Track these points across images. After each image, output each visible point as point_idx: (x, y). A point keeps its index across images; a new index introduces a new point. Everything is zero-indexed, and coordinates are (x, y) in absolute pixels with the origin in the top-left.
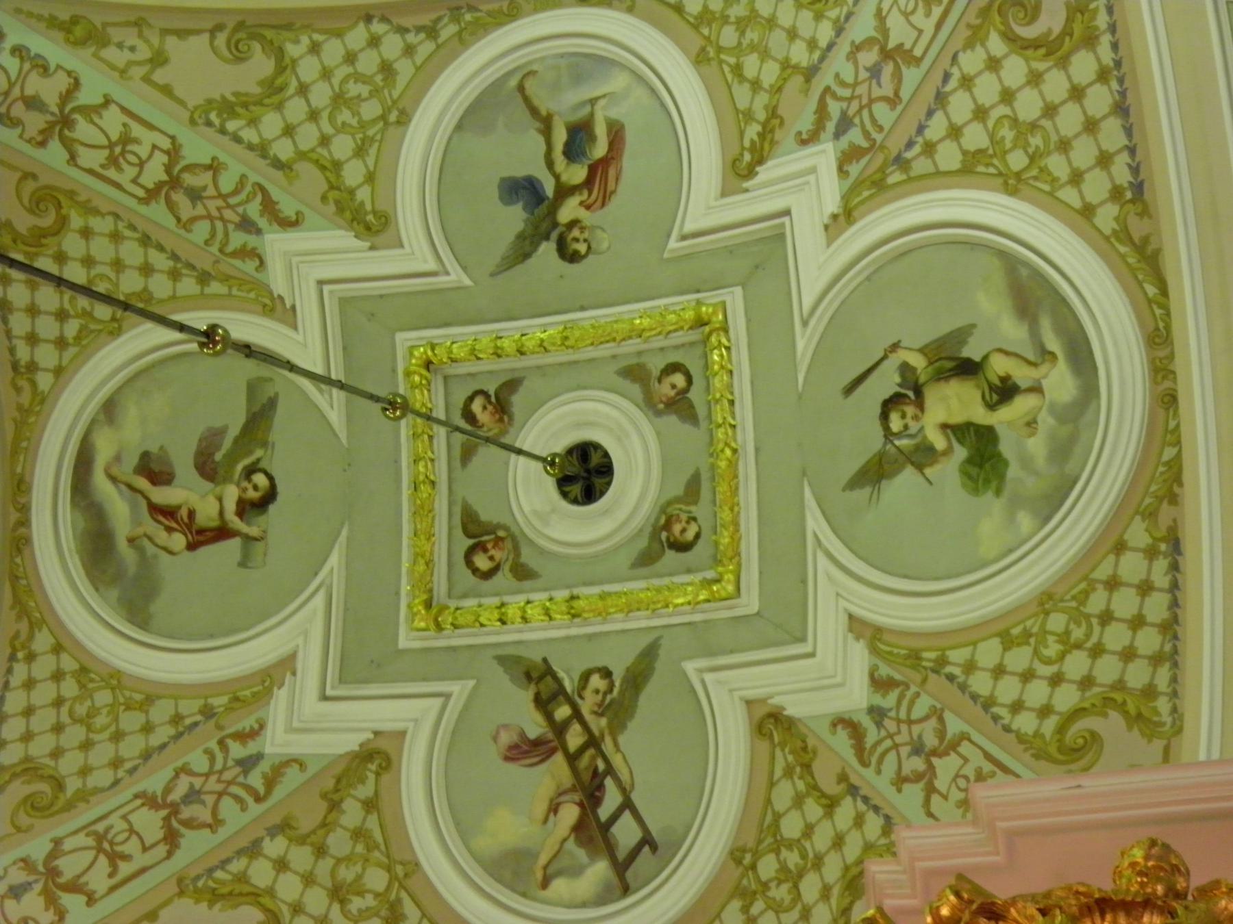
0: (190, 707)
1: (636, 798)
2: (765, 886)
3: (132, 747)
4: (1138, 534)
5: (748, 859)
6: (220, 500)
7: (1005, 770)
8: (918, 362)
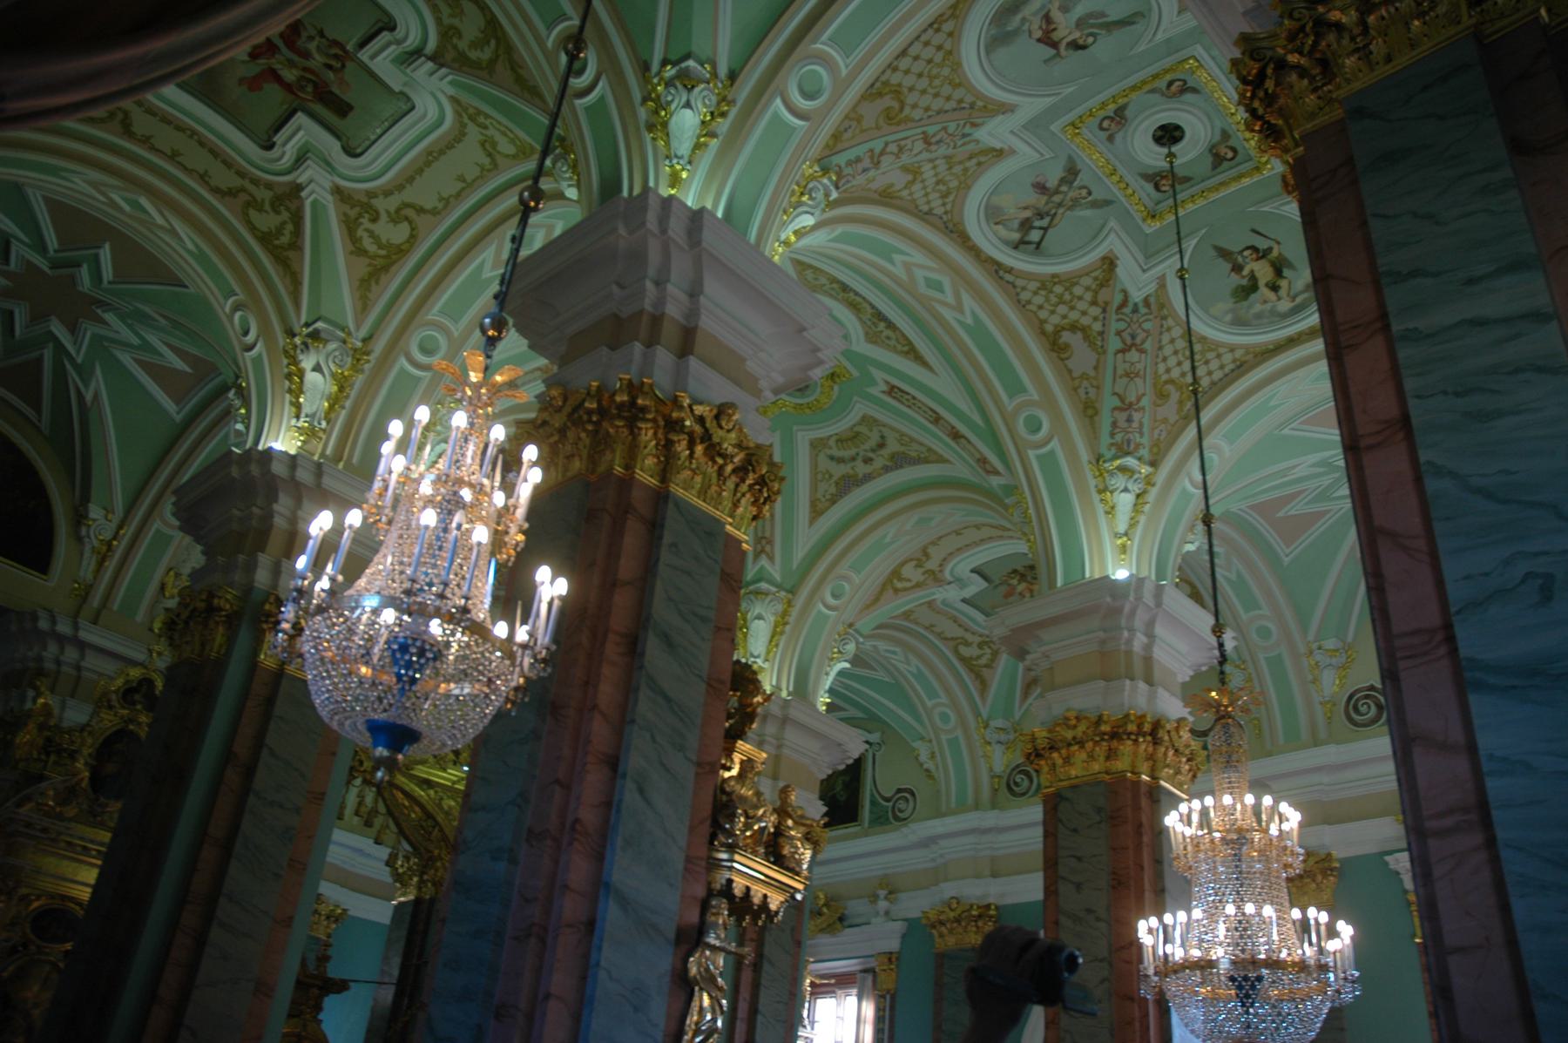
0: (969, 99)
1: (1050, 231)
2: (1051, 292)
3: (938, 104)
4: (1239, 354)
5: (1056, 280)
6: (1070, 33)
7: (1145, 382)
8: (1275, 253)
